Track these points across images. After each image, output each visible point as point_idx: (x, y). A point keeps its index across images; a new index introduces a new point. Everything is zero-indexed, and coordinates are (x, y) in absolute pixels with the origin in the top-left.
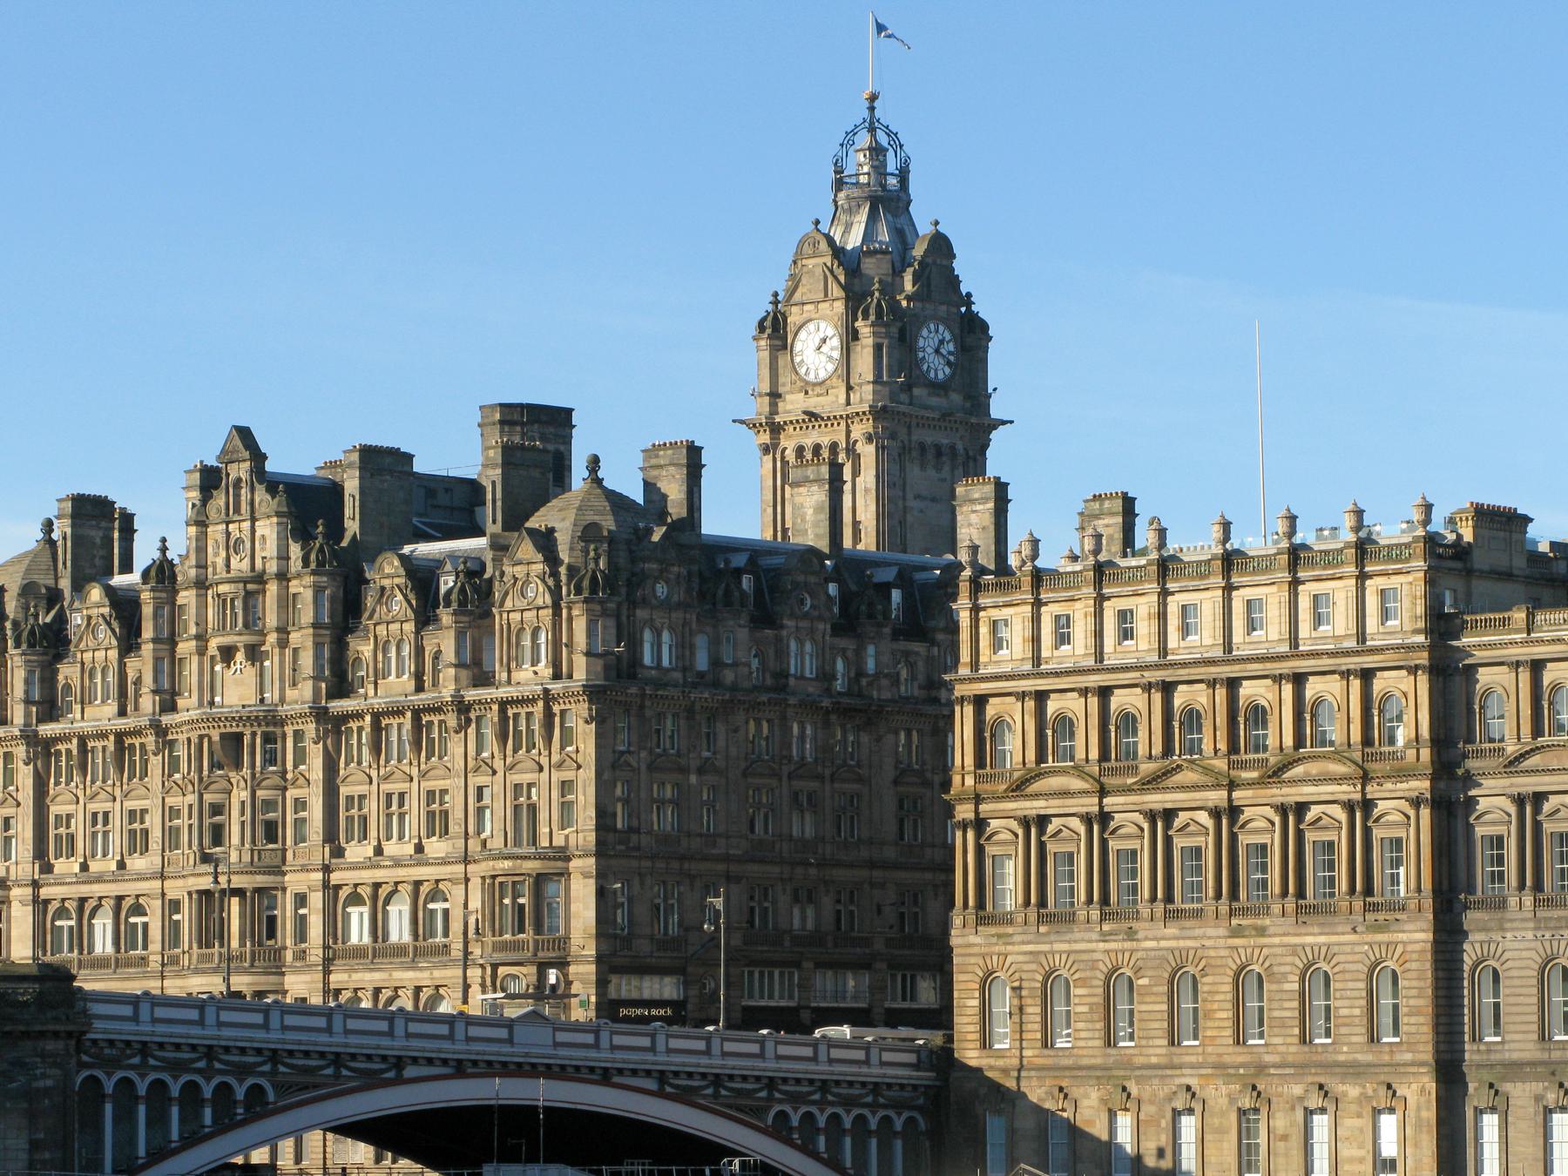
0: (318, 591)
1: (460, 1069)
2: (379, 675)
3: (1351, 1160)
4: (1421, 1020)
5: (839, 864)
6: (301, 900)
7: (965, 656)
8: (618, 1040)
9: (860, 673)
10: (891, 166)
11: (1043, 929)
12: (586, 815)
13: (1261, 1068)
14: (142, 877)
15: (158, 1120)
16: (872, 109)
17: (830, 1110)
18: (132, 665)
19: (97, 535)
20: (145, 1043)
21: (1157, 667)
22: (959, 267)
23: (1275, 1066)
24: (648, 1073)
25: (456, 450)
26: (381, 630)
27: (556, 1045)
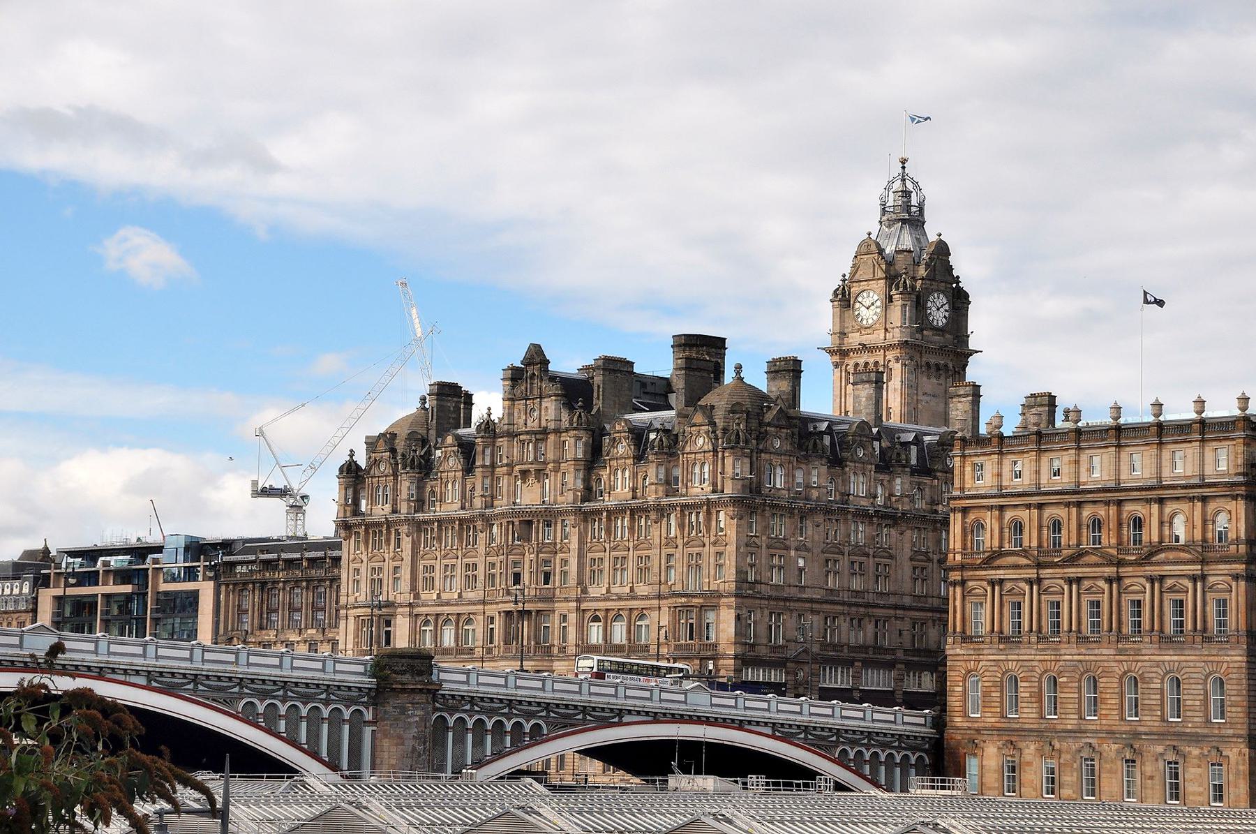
0: (578, 439)
1: (657, 718)
2: (612, 488)
3: (1194, 794)
4: (1239, 709)
5: (877, 606)
6: (564, 617)
7: (957, 484)
8: (748, 704)
9: (891, 495)
10: (914, 201)
11: (1001, 646)
12: (730, 572)
13: (1136, 735)
14: (472, 603)
15: (479, 743)
16: (903, 168)
17: (873, 750)
18: (470, 479)
19: (451, 405)
20: (472, 697)
22: (952, 260)
23: (1146, 734)
24: (766, 724)
25: (657, 362)
26: (614, 463)
27: (712, 705)
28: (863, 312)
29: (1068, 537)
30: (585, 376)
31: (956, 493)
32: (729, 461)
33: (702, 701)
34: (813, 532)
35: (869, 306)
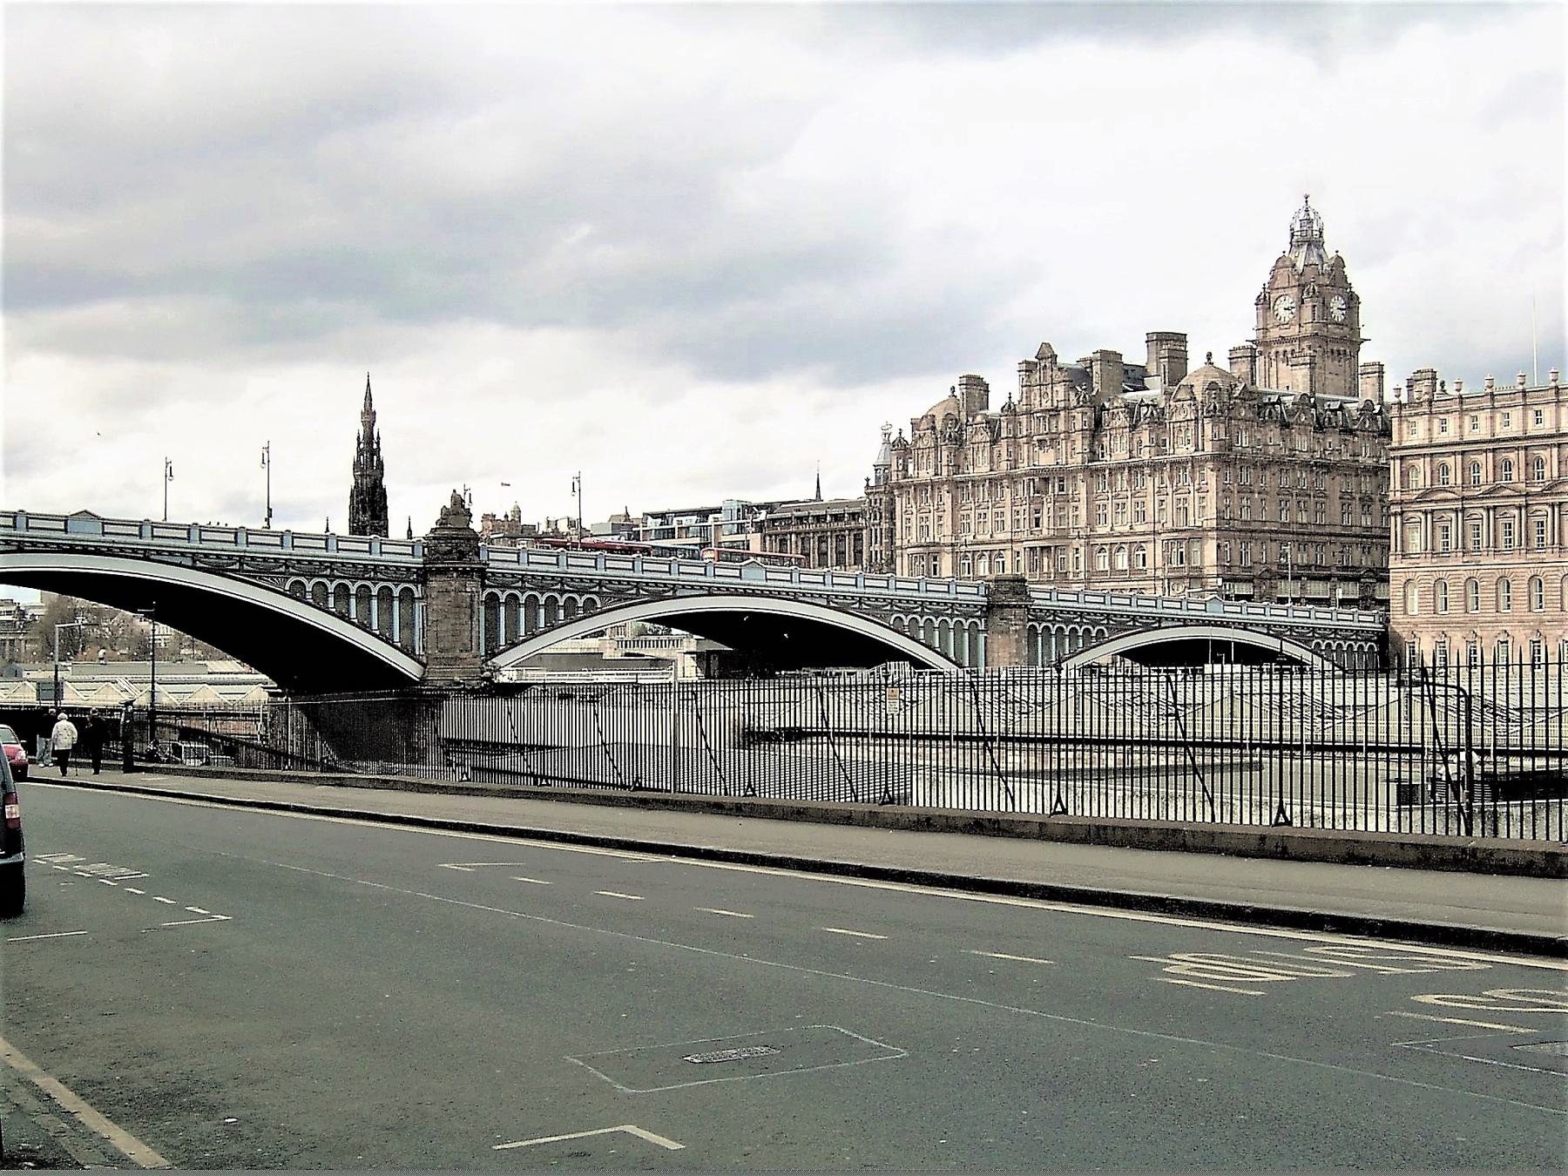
0: (1084, 413)
12: (1211, 512)
13: (1542, 622)
15: (1060, 644)
21: (1490, 441)
25: (1136, 354)
28: (1282, 312)
29: (1485, 475)
30: (1081, 366)
31: (1395, 445)
32: (1208, 428)
33: (1216, 610)
34: (1270, 480)
35: (1284, 307)
